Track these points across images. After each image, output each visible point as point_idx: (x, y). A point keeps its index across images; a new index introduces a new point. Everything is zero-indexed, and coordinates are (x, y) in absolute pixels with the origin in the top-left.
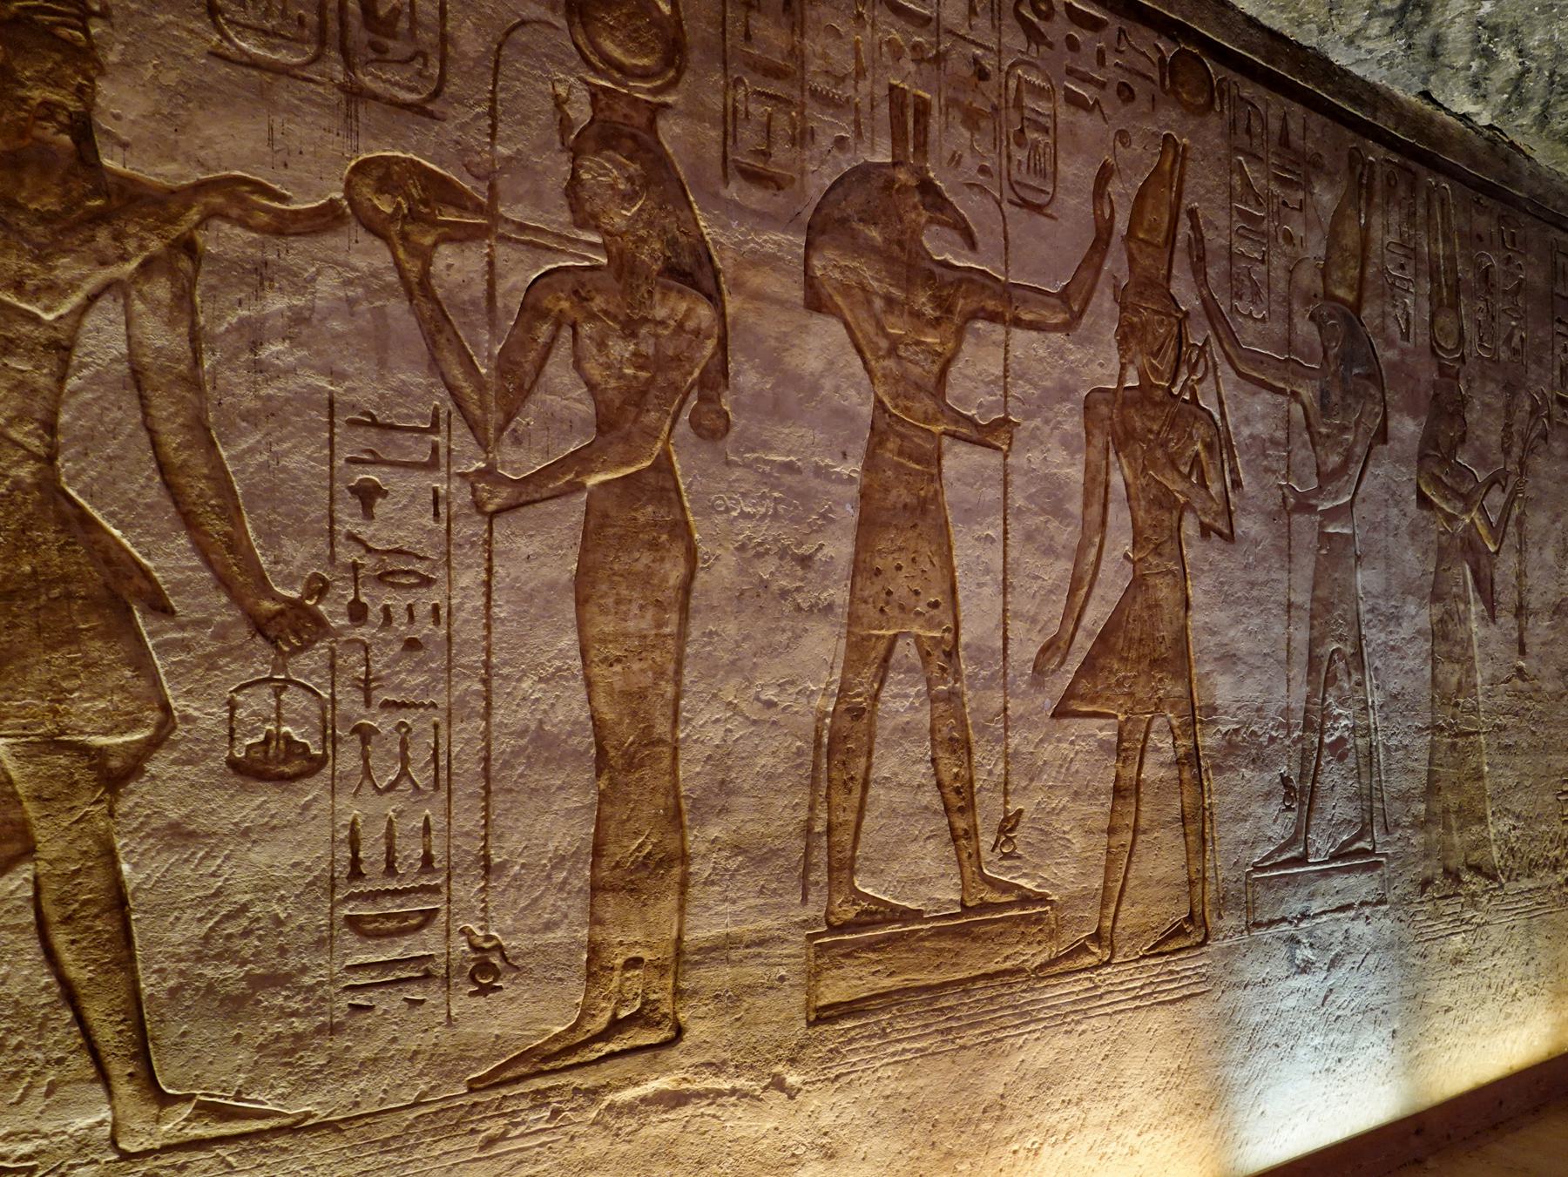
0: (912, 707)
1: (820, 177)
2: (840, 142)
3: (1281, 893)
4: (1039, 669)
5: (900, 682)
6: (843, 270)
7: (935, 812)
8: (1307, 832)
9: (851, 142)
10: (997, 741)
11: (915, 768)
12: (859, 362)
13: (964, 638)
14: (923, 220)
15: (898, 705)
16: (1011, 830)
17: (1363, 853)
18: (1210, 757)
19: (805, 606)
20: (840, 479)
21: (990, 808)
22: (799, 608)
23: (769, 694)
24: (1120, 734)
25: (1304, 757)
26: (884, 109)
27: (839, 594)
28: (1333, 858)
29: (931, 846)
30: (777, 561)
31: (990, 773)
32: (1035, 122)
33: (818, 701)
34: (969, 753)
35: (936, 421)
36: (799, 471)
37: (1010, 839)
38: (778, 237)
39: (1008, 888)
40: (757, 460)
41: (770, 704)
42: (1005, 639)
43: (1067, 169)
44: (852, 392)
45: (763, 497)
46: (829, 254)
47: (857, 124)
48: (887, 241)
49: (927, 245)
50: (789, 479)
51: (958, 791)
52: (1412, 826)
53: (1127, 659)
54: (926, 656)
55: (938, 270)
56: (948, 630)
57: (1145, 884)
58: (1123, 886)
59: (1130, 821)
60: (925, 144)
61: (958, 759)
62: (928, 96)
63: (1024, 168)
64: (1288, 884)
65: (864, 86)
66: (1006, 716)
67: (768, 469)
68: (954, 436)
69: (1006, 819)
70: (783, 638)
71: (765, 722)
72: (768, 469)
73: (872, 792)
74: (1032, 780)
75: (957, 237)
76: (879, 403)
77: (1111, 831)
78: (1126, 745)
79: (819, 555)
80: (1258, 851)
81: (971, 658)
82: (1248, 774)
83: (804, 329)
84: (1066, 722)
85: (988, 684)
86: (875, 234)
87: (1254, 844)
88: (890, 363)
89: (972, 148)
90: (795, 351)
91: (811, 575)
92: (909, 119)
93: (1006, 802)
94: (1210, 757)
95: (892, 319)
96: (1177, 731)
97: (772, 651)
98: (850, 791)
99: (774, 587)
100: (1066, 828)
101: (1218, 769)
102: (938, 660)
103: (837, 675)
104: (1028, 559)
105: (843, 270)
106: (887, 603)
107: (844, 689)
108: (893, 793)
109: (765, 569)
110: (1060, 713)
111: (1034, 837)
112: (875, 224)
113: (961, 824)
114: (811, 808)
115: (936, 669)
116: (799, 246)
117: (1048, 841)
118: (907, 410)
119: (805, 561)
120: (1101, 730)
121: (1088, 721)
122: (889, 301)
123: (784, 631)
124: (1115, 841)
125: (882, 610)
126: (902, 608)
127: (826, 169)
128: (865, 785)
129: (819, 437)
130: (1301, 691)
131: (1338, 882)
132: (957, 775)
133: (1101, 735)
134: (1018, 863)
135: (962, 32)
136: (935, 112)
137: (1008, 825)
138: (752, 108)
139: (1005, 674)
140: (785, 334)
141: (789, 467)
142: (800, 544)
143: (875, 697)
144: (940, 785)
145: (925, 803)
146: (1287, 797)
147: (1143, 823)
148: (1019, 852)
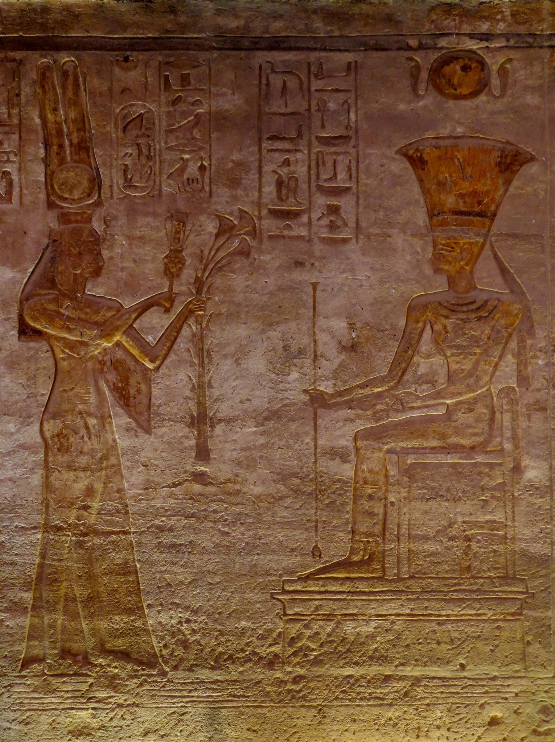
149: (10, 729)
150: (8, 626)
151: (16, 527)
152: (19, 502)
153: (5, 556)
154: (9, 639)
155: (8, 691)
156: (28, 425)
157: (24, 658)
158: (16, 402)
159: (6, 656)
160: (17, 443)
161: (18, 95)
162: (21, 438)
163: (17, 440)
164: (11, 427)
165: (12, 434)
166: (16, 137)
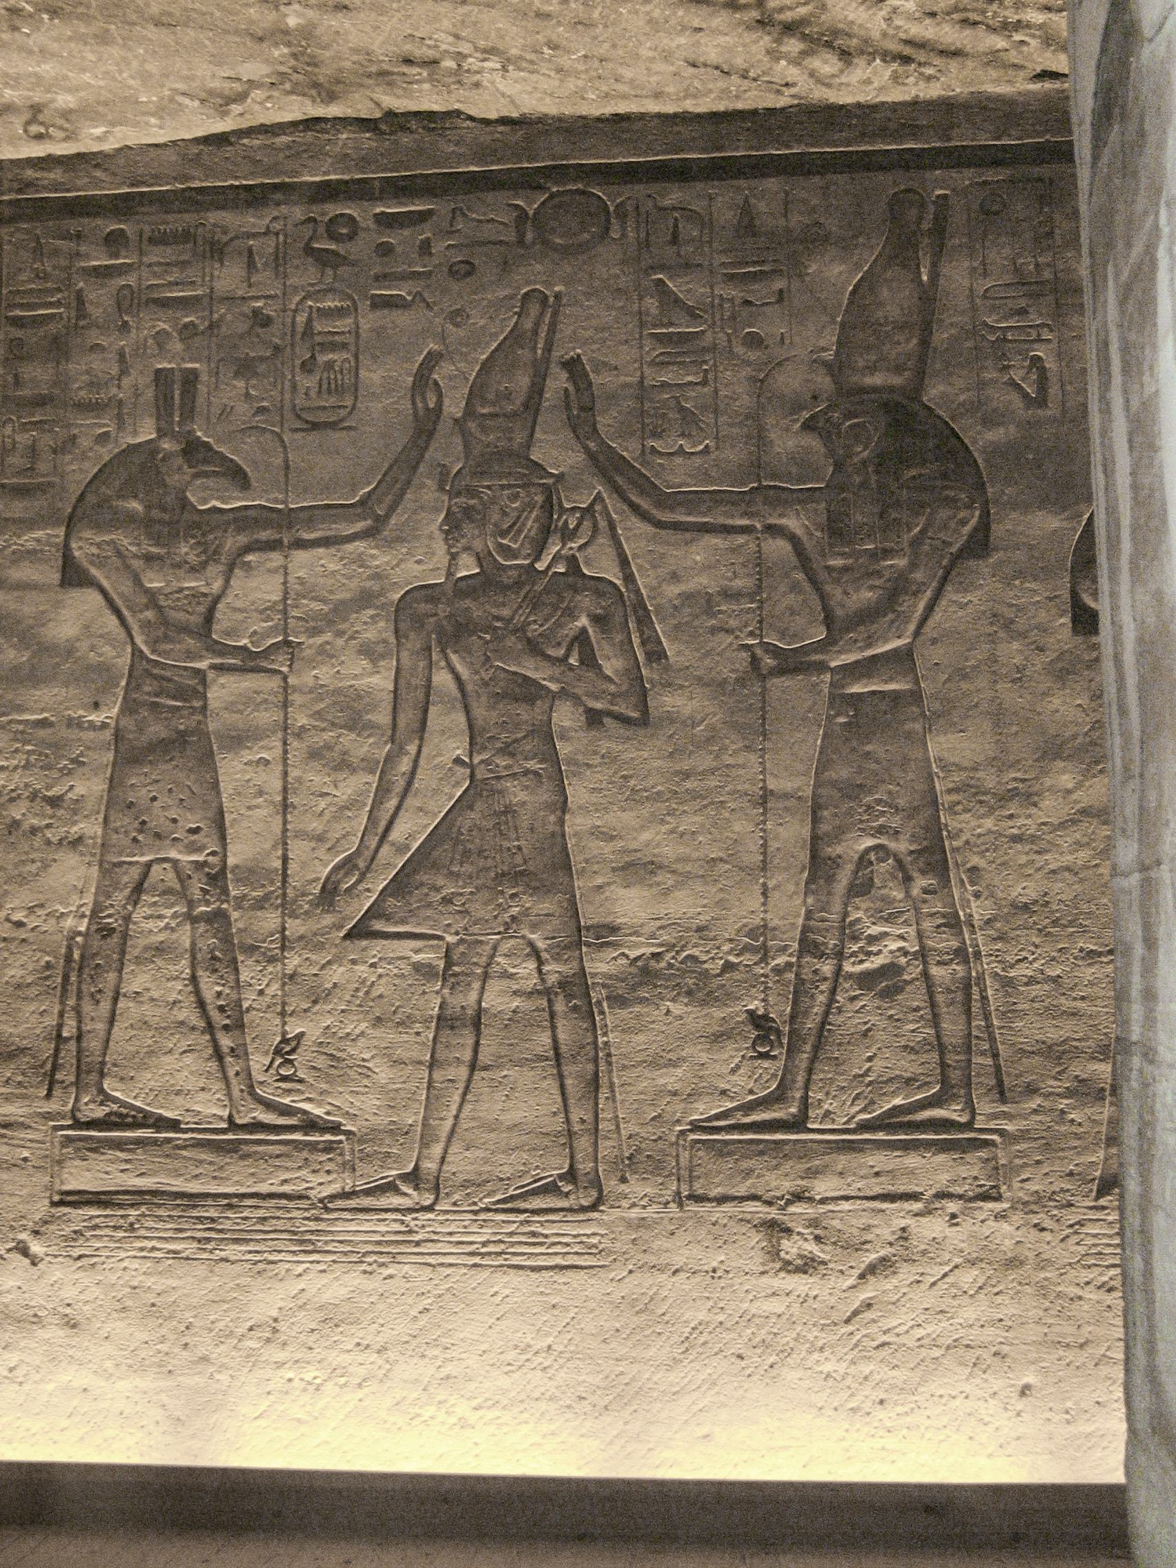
0: (167, 927)
1: (78, 472)
2: (103, 438)
3: (746, 1164)
4: (329, 894)
5: (155, 903)
6: (99, 545)
7: (193, 1028)
8: (807, 1088)
9: (113, 435)
10: (272, 960)
11: (170, 985)
12: (113, 621)
13: (231, 861)
14: (187, 478)
15: (151, 924)
16: (293, 1051)
17: (947, 1125)
18: (604, 986)
19: (55, 840)
20: (92, 726)
21: (265, 1028)
22: (49, 843)
23: (17, 916)
24: (448, 955)
25: (800, 991)
26: (150, 394)
27: (91, 828)
28: (865, 1127)
29: (189, 1059)
30: (27, 803)
31: (261, 993)
32: (331, 343)
33: (69, 922)
34: (237, 970)
35: (201, 658)
36: (51, 725)
37: (291, 1062)
38: (39, 534)
39: (286, 1111)
40: (11, 722)
41: (19, 924)
42: (285, 860)
43: (372, 376)
44: (107, 649)
45: (17, 751)
46: (87, 534)
47: (120, 417)
48: (148, 508)
49: (192, 499)
50: (42, 733)
51: (221, 1009)
52: (1069, 1093)
53: (458, 875)
54: (183, 879)
55: (207, 517)
56: (213, 853)
57: (492, 1127)
58: (455, 1125)
59: (467, 1055)
60: (192, 410)
61: (222, 977)
62: (197, 365)
63: (313, 394)
64: (762, 1153)
65: (126, 382)
66: (284, 938)
67: (21, 727)
68: (219, 668)
69: (285, 1041)
70: (33, 868)
71: (14, 939)
72: (21, 727)
73: (120, 1005)
74: (315, 1002)
75: (223, 482)
76: (137, 653)
77: (433, 1064)
78: (456, 969)
79: (70, 795)
80: (701, 1107)
81: (238, 880)
82: (677, 1009)
83: (58, 604)
84: (364, 943)
85: (260, 904)
86: (135, 506)
87: (693, 1095)
88: (149, 614)
89: (247, 395)
90: (51, 625)
91: (61, 812)
92: (175, 394)
93: (284, 1023)
94: (604, 986)
95: (150, 574)
96: (544, 955)
97: (23, 880)
98: (98, 1002)
99: (26, 826)
100: (367, 1056)
101: (618, 1001)
102: (196, 887)
103: (89, 899)
104: (317, 778)
105: (99, 545)
106: (141, 831)
107: (94, 913)
108: (146, 1007)
109: (16, 812)
110: (360, 932)
111: (321, 1062)
112: (136, 497)
113: (226, 1042)
114: (61, 1015)
115: (198, 892)
116: (57, 536)
117: (336, 1066)
118: (166, 654)
119: (55, 802)
120: (417, 952)
121: (396, 943)
122: (149, 558)
123: (33, 861)
124: (437, 1075)
125: (135, 840)
126: (158, 836)
127: (87, 465)
128: (115, 1000)
129: (73, 691)
130: (788, 908)
131: (878, 1160)
132: (219, 994)
133: (417, 958)
134: (298, 1086)
135: (240, 293)
136: (204, 377)
137: (286, 1049)
138: (18, 438)
139: (284, 895)
140: (43, 612)
141: (43, 723)
142: (48, 788)
143: (127, 919)
144: (201, 1004)
145: (181, 1018)
146: (761, 1039)
147: (484, 1058)
148: (301, 1074)
149: (1080, 1298)
150: (1072, 1121)
151: (1081, 950)
152: (1084, 907)
153: (1063, 1000)
154: (1076, 1143)
155: (1076, 1233)
156: (1094, 776)
157: (1101, 1178)
158: (1075, 737)
159: (1071, 1174)
160: (1078, 807)
161: (1050, 234)
162: (1083, 798)
163: (1076, 802)
164: (1067, 780)
165: (1069, 792)
166: (1050, 298)
